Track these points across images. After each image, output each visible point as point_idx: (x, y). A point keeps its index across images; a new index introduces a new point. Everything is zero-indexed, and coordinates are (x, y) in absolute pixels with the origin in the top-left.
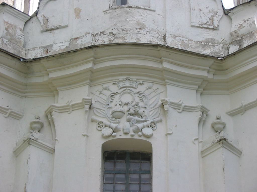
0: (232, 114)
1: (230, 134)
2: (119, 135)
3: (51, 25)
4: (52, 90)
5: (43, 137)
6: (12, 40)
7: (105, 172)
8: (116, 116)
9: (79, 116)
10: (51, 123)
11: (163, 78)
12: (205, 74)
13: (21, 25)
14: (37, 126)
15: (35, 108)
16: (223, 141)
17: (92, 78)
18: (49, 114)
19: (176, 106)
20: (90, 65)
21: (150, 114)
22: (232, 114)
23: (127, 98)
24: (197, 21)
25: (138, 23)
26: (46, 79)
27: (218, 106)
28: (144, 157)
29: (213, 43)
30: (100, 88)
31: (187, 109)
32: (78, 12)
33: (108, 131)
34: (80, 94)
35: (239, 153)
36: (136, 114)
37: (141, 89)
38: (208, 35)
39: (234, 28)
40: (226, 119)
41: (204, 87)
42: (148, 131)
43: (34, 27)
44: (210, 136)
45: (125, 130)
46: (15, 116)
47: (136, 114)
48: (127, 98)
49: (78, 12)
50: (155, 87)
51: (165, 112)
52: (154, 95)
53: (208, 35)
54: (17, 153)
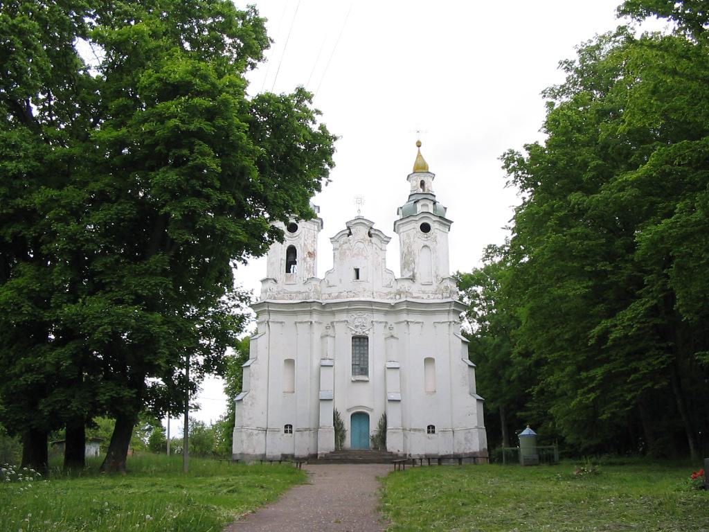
0: (396, 323)
1: (394, 332)
2: (358, 334)
3: (330, 284)
4: (333, 313)
5: (330, 332)
6: (316, 291)
7: (352, 345)
8: (357, 327)
9: (343, 325)
10: (333, 327)
11: (372, 311)
12: (387, 309)
13: (319, 284)
14: (326, 328)
15: (328, 319)
16: (392, 336)
17: (348, 311)
18: (332, 323)
19: (376, 322)
20: (347, 307)
21: (368, 325)
22: (396, 323)
23: (360, 320)
24: (385, 284)
25: (364, 288)
26: (330, 310)
27: (391, 319)
28: (368, 339)
29: (390, 293)
30: (350, 315)
31: (380, 322)
32: (341, 280)
33: (354, 333)
34: (344, 317)
35: (397, 339)
36: (364, 326)
37: (365, 316)
38: (389, 290)
39: (398, 288)
40: (394, 325)
41: (387, 313)
42: (367, 332)
43: (324, 285)
44: (387, 331)
45: (359, 332)
46: (320, 323)
47: (364, 326)
48: (360, 320)
49: (341, 280)
50: (370, 315)
51: (373, 325)
52: (367, 318)
53: (389, 290)
54: (322, 337)
